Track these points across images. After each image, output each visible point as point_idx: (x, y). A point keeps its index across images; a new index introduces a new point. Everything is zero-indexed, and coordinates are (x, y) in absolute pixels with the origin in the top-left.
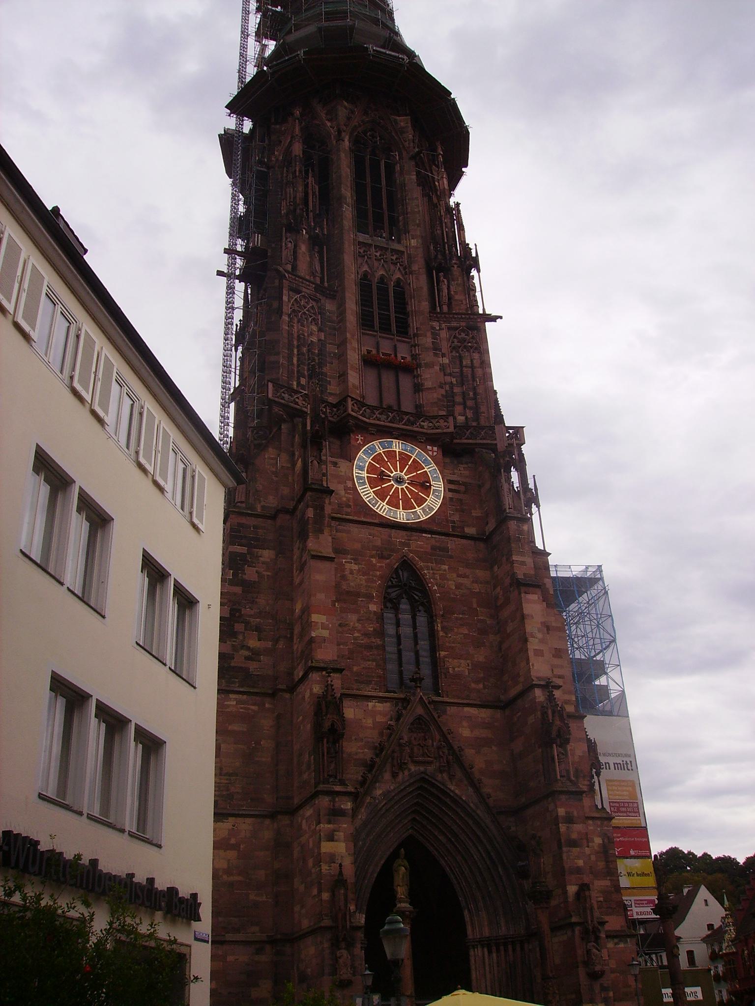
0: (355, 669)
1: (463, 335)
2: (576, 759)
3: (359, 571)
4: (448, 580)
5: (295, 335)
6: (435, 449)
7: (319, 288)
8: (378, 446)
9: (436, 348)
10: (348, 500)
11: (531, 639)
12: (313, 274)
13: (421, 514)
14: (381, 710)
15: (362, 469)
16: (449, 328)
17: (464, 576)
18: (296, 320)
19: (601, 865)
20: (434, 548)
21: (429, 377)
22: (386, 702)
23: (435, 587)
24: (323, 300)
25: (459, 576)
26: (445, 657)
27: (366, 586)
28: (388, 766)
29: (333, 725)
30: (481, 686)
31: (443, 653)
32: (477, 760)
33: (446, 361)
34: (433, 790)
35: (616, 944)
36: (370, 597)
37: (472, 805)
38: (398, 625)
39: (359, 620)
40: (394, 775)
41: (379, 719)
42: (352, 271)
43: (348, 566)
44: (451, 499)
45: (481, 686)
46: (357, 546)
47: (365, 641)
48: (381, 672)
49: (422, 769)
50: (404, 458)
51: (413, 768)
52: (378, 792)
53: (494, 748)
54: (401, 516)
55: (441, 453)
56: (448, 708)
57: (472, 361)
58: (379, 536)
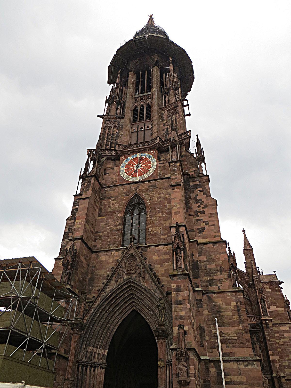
0: (109, 240)
1: (173, 111)
2: (221, 262)
3: (116, 203)
4: (154, 197)
5: (107, 134)
6: (154, 151)
7: (117, 117)
8: (131, 158)
9: (162, 119)
10: (116, 179)
11: (173, 208)
12: (117, 114)
13: (146, 176)
14: (117, 255)
15: (123, 167)
16: (167, 111)
17: (163, 193)
18: (107, 129)
19: (236, 317)
20: (149, 187)
21: (155, 129)
22: (120, 251)
23: (148, 201)
24: (119, 120)
25: (160, 194)
26: (150, 227)
27: (118, 208)
28: (114, 278)
29: (68, 261)
30: (166, 236)
31: (149, 226)
32: (160, 270)
33: (166, 121)
34: (137, 286)
35: (246, 366)
36: (119, 211)
37: (153, 291)
38: (132, 219)
39: (113, 221)
40: (116, 281)
41: (116, 258)
42: (129, 107)
43: (111, 202)
44: (160, 167)
45: (166, 236)
46: (117, 194)
47: (115, 228)
48: (119, 239)
49: (130, 277)
50: (141, 158)
51: (125, 277)
52: (107, 290)
53: (170, 263)
54: (137, 179)
55: (157, 151)
56: (148, 249)
57: (175, 117)
58: (125, 189)
